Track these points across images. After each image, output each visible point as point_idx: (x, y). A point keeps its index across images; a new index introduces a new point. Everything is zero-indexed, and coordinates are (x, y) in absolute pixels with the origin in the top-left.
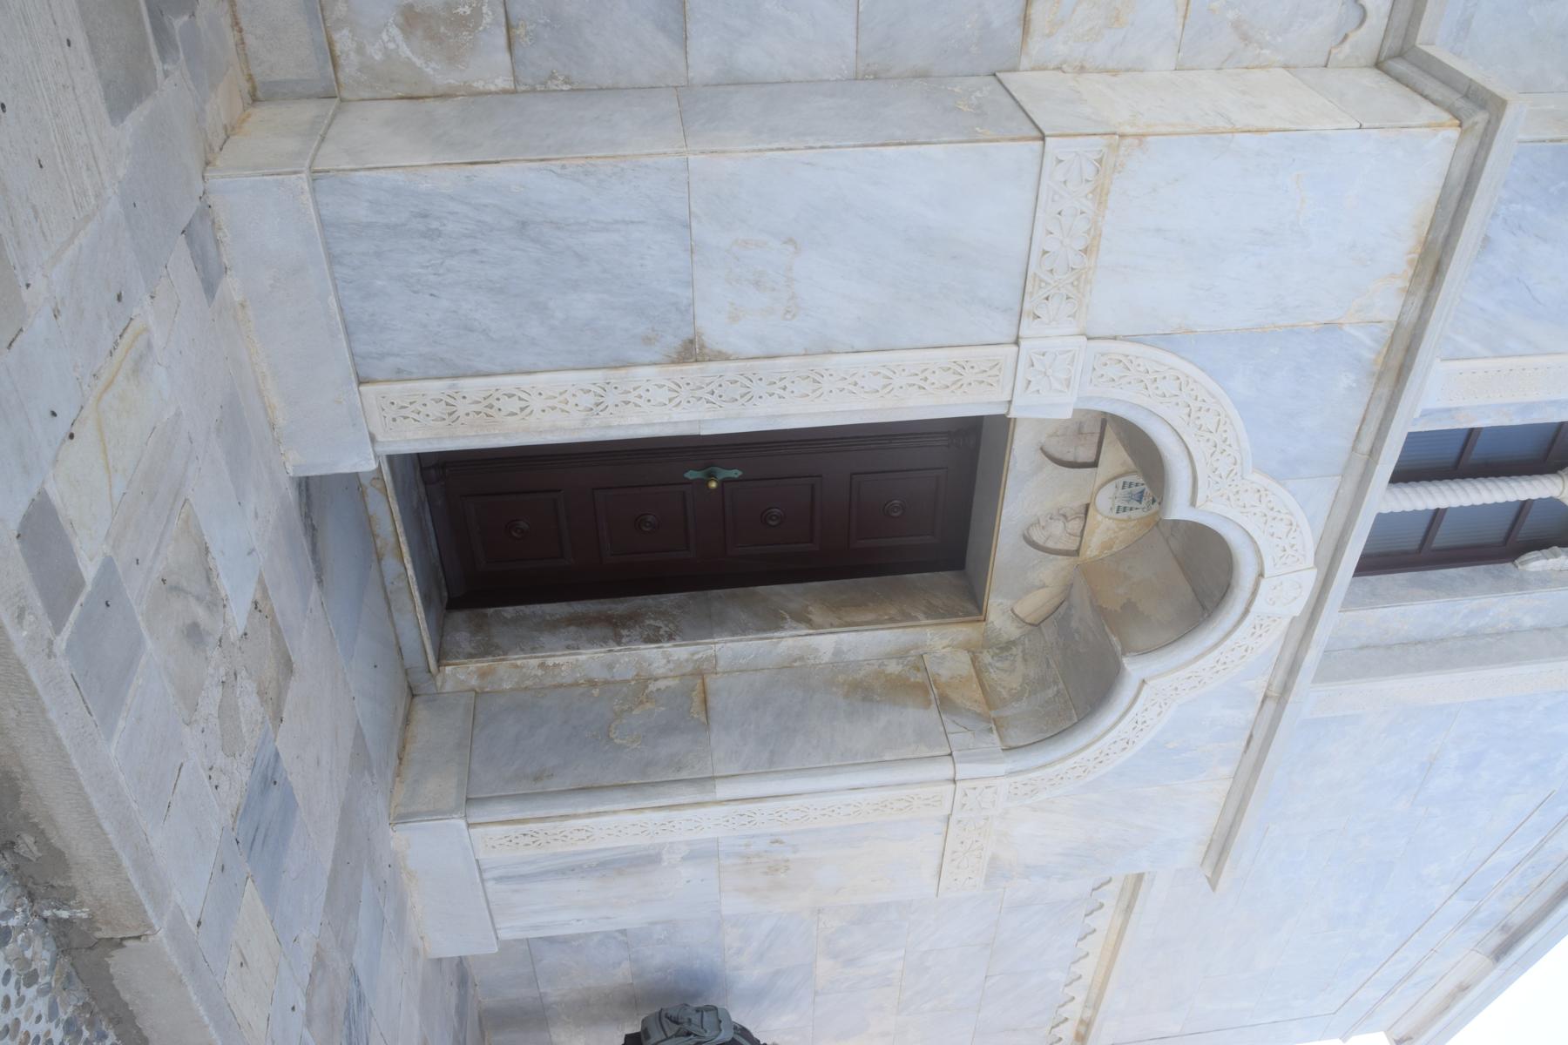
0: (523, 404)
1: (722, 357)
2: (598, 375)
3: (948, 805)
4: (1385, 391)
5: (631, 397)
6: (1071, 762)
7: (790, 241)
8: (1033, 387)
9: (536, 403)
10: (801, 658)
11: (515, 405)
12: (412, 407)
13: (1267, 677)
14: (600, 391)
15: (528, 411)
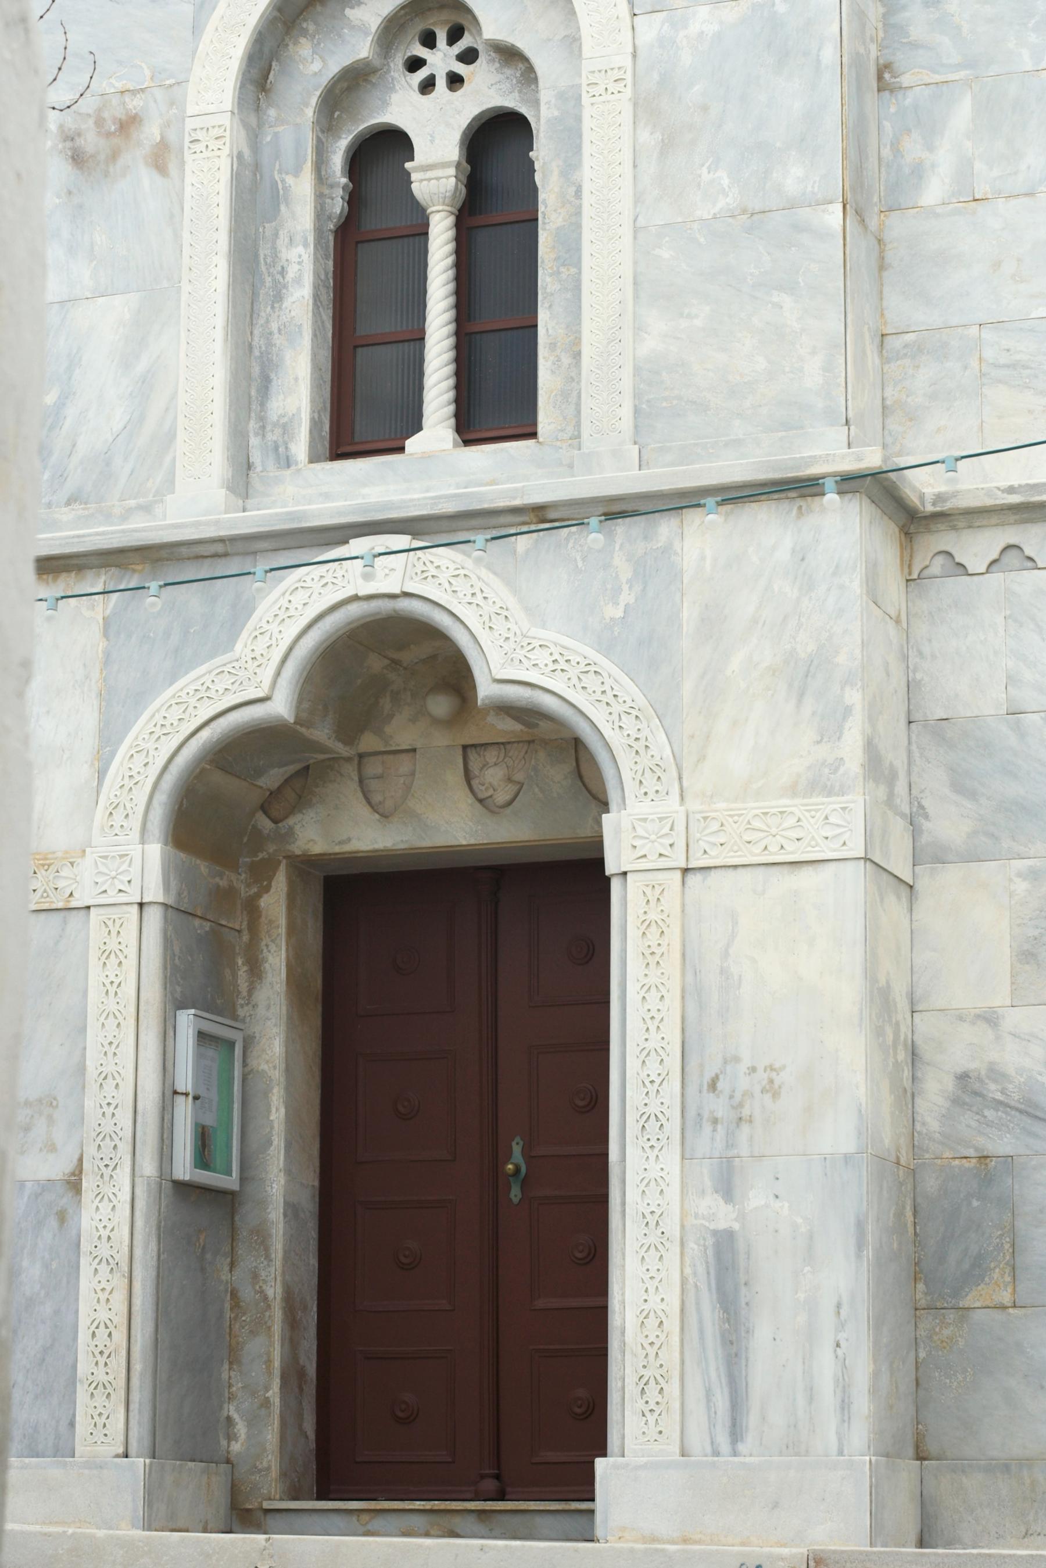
0: (102, 1325)
1: (81, 1160)
2: (83, 1261)
3: (661, 876)
5: (105, 1234)
6: (607, 732)
9: (103, 1315)
11: (102, 1332)
12: (96, 1418)
14: (97, 1260)
15: (108, 1323)
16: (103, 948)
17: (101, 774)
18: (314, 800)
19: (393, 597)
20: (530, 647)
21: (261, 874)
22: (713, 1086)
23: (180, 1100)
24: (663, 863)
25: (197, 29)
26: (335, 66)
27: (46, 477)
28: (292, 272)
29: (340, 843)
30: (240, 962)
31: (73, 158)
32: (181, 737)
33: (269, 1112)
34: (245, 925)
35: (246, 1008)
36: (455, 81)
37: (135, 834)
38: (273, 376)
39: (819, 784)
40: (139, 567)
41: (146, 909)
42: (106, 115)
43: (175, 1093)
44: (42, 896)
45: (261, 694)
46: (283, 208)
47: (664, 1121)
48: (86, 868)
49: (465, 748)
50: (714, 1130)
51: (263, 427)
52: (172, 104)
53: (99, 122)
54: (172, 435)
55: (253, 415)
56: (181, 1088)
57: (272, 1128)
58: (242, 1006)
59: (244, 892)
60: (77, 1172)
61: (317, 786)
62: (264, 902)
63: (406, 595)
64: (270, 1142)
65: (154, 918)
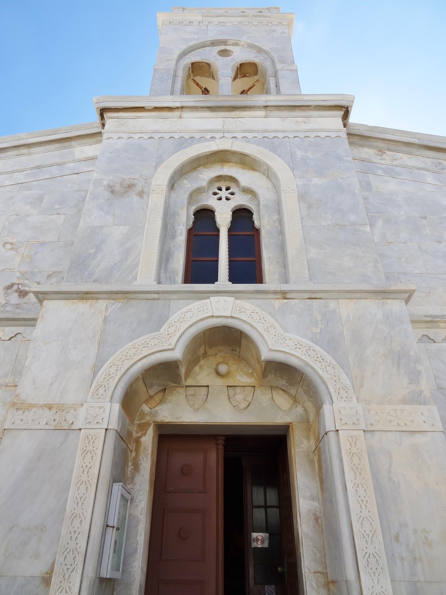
1: (53, 564)
3: (355, 433)
4: (134, 296)
6: (321, 373)
7: (11, 529)
8: (100, 421)
10: (317, 519)
13: (273, 301)
16: (85, 449)
17: (95, 374)
18: (167, 401)
19: (227, 317)
20: (285, 339)
21: (143, 427)
22: (397, 538)
23: (110, 530)
24: (354, 427)
25: (156, 168)
26: (195, 186)
27: (86, 273)
28: (179, 232)
29: (177, 418)
30: (130, 464)
31: (111, 192)
32: (134, 361)
33: (137, 536)
34: (134, 449)
35: (131, 485)
36: (227, 199)
37: (108, 399)
38: (170, 258)
39: (416, 399)
40: (122, 301)
41: (108, 431)
42: (124, 183)
43: (108, 526)
44: (58, 423)
45: (170, 347)
46: (176, 216)
47: (378, 558)
48: (82, 412)
49: (228, 386)
50: (403, 565)
51: (166, 272)
52: (146, 183)
53: (121, 184)
54: (137, 265)
55: (162, 268)
56: (110, 524)
57: (137, 544)
58: (129, 484)
59: (135, 435)
60: (49, 572)
61: (168, 396)
62: (142, 439)
63: (232, 317)
64: (136, 552)
65: (111, 437)
